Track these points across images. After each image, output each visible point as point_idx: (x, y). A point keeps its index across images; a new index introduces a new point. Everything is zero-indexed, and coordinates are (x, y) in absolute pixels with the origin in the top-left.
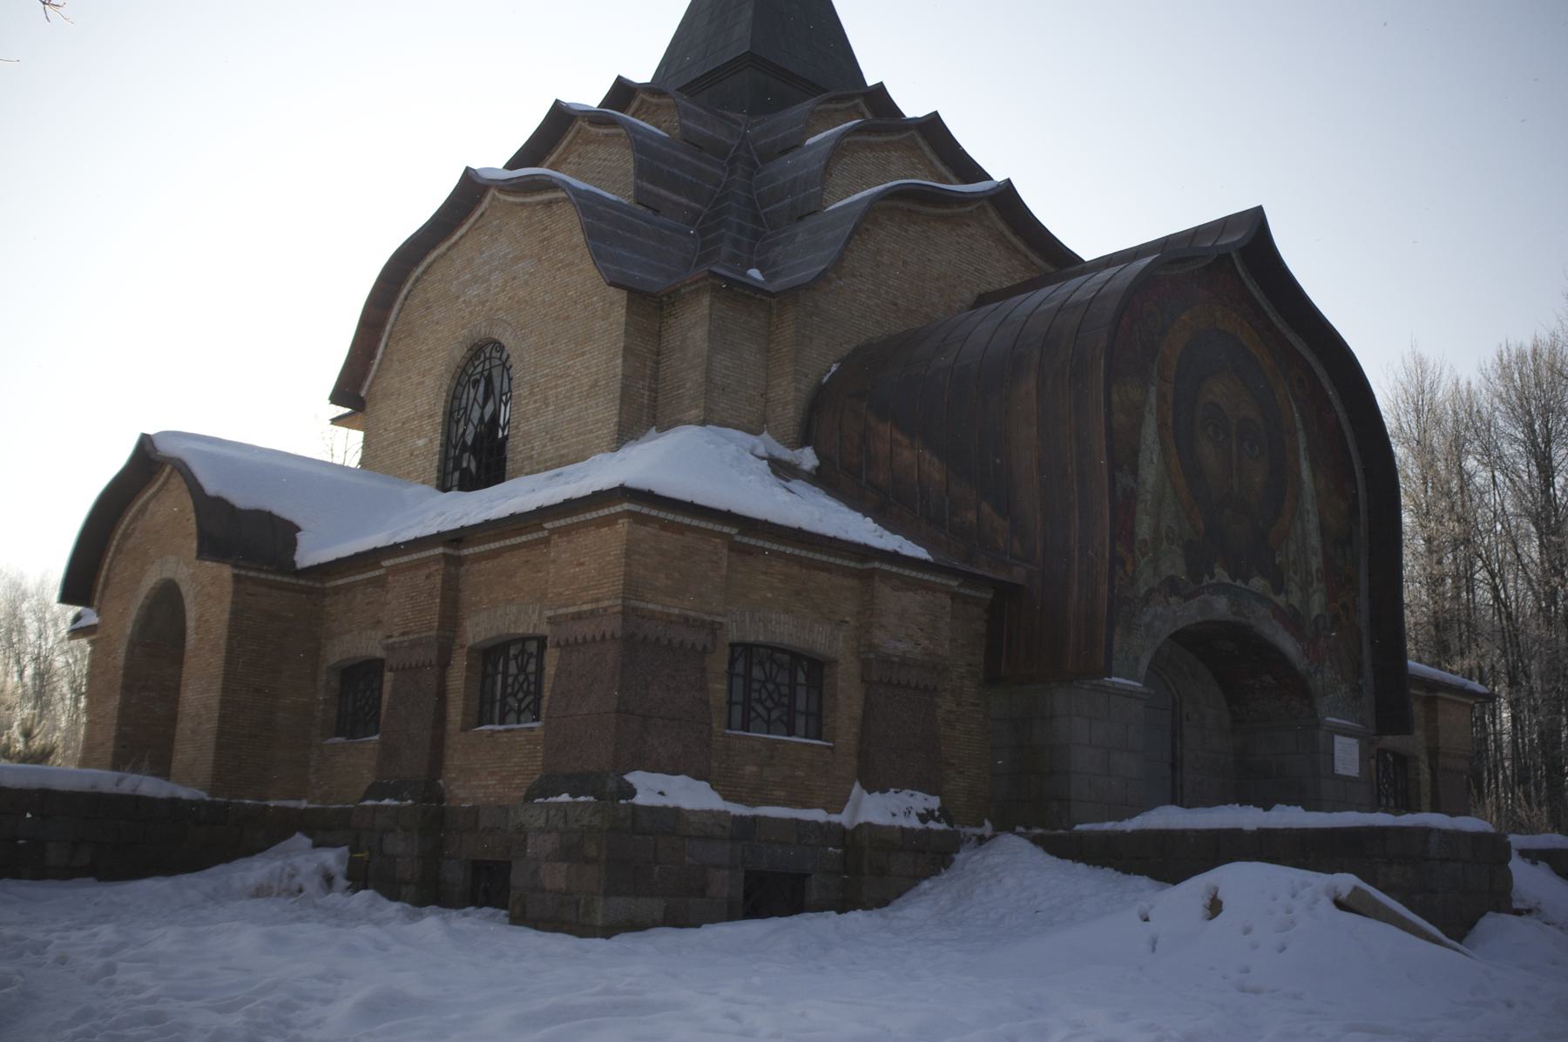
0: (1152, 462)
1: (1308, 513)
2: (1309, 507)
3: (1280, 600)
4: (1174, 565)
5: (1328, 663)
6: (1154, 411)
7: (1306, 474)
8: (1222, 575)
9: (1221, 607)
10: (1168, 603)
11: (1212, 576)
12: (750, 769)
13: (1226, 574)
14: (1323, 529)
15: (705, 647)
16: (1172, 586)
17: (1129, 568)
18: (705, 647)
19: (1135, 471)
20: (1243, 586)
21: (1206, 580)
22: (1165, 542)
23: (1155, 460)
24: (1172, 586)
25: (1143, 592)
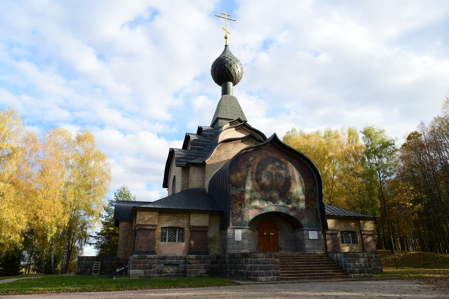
3: (290, 206)
15: (154, 229)
17: (243, 205)
18: (154, 229)
19: (244, 187)
20: (277, 204)
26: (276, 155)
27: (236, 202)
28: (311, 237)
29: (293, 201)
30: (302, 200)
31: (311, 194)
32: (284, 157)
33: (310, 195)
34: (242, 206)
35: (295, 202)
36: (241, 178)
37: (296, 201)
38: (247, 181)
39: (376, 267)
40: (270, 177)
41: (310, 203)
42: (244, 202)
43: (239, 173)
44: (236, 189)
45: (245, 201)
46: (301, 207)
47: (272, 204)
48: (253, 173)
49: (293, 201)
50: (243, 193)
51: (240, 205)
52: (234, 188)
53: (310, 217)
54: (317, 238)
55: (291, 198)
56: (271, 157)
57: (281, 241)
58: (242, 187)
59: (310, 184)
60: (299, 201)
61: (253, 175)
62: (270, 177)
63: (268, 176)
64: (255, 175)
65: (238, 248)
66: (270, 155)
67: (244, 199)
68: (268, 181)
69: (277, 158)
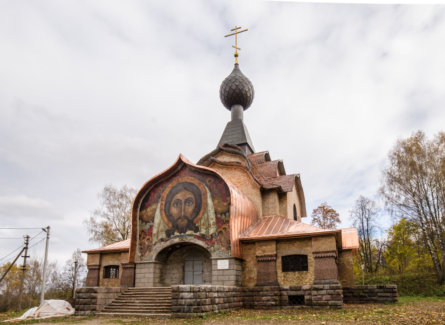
0: (158, 218)
1: (210, 211)
2: (210, 209)
3: (198, 234)
4: (163, 235)
5: (216, 244)
6: (159, 208)
7: (210, 201)
8: (177, 234)
9: (177, 240)
10: (161, 244)
11: (174, 235)
12: (106, 283)
13: (178, 233)
14: (216, 213)
16: (162, 240)
17: (151, 240)
19: (153, 222)
20: (184, 234)
21: (172, 236)
22: (160, 232)
23: (159, 217)
24: (162, 240)
25: (154, 243)
26: (188, 179)
27: (144, 238)
28: (219, 267)
29: (202, 228)
30: (213, 225)
31: (225, 216)
32: (197, 178)
33: (224, 217)
34: (150, 241)
35: (204, 228)
36: (151, 212)
37: (206, 227)
38: (156, 215)
39: (329, 302)
40: (179, 205)
41: (224, 226)
42: (151, 236)
43: (149, 208)
44: (146, 224)
45: (153, 235)
46: (211, 233)
47: (178, 234)
48: (162, 204)
49: (202, 228)
50: (151, 227)
51: (149, 239)
52: (144, 223)
53: (220, 244)
54: (227, 267)
55: (199, 224)
56: (183, 183)
57: (206, 273)
58: (151, 221)
59: (225, 204)
60: (209, 226)
61: (162, 206)
62: (179, 205)
63: (177, 205)
64: (164, 207)
65: (144, 282)
66: (181, 181)
67: (152, 233)
68: (177, 210)
69: (189, 181)
